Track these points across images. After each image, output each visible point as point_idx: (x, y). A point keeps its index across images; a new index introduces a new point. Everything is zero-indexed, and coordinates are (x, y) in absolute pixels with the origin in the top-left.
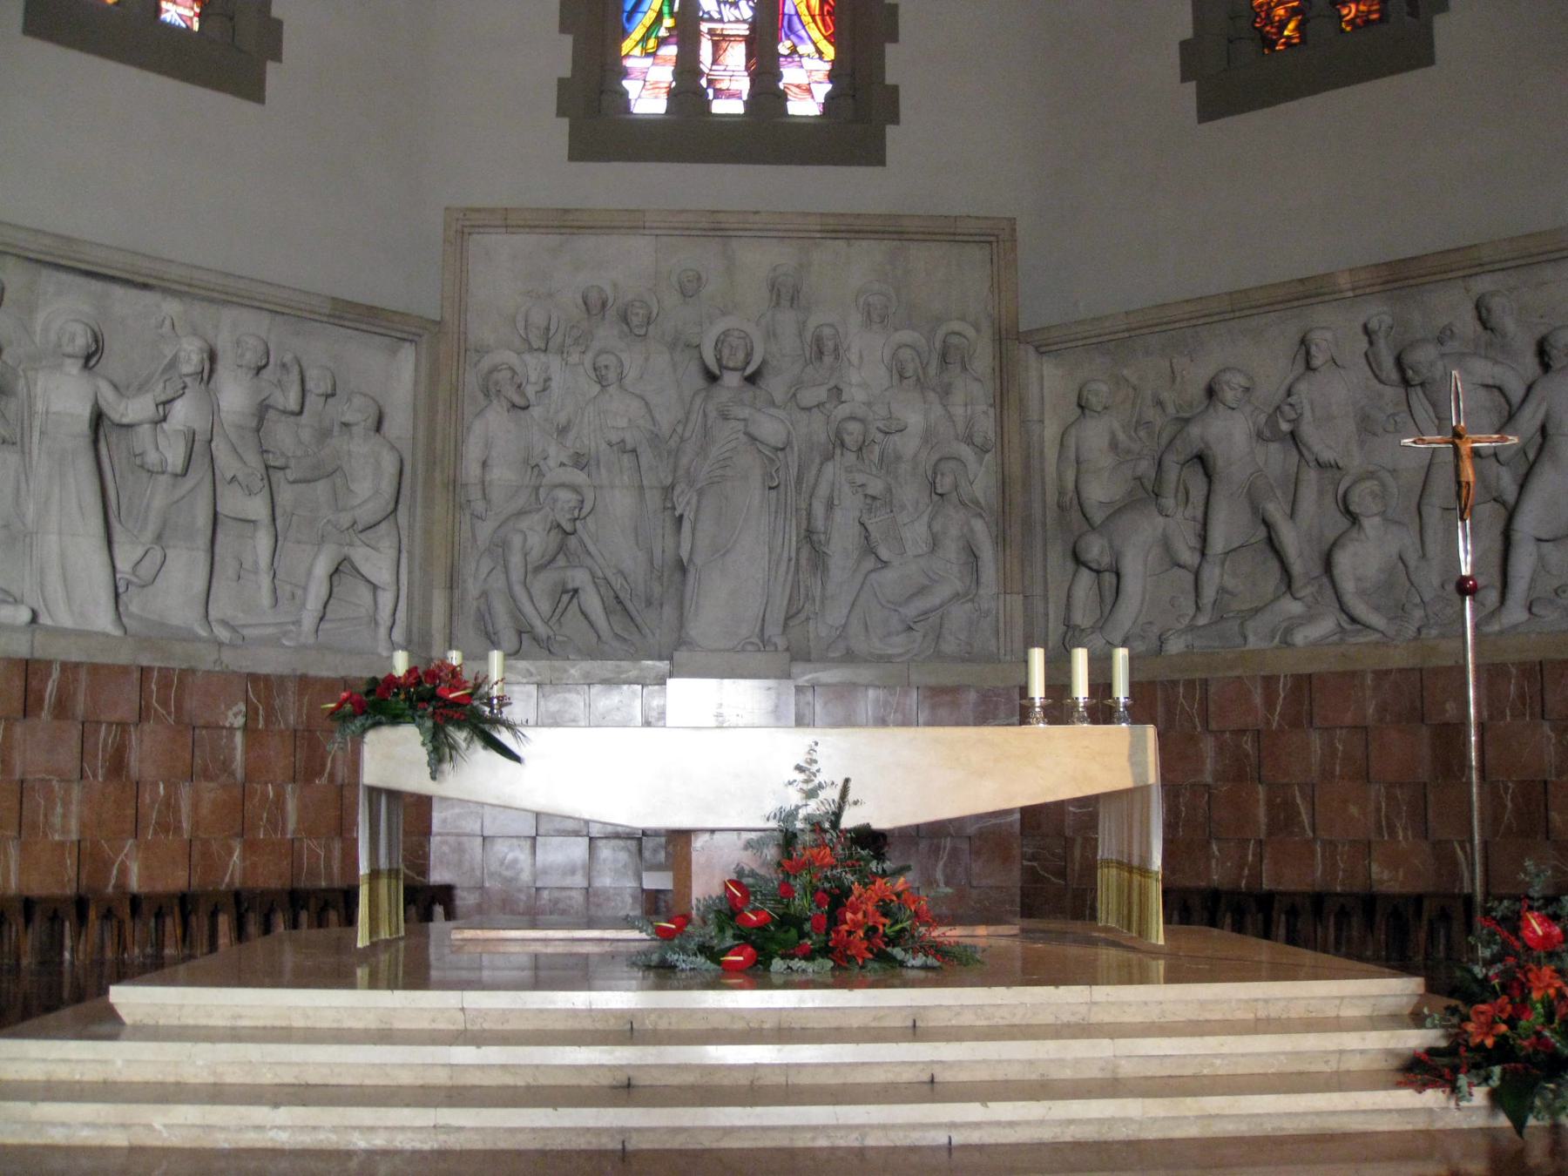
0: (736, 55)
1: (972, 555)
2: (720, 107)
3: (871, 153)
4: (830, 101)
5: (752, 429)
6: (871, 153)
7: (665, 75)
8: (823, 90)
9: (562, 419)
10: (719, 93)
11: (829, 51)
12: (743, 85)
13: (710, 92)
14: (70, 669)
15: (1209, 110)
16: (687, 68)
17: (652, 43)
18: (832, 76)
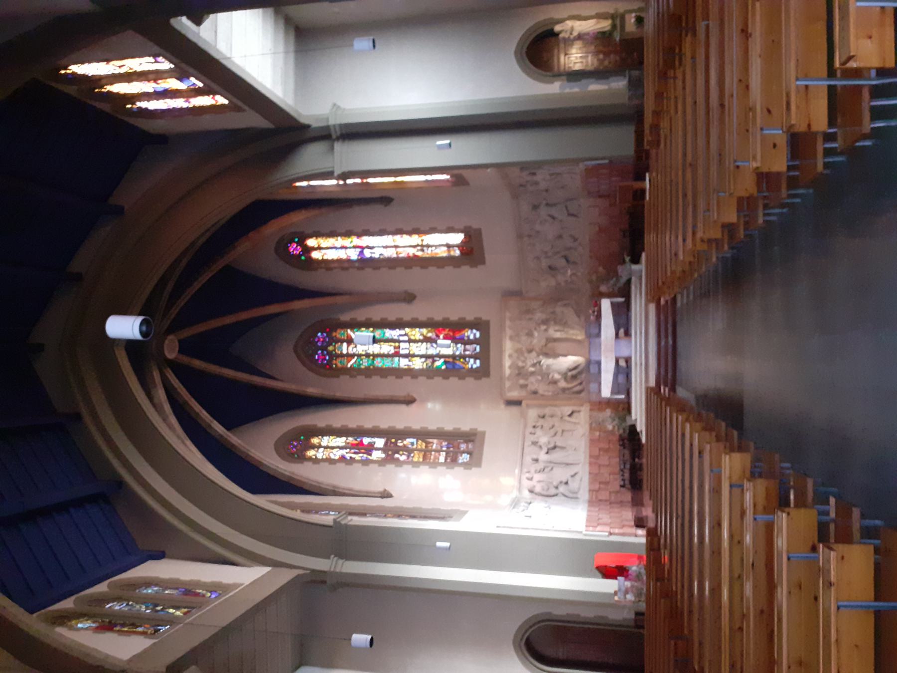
0: (468, 347)
1: (565, 305)
2: (478, 349)
3: (487, 323)
4: (477, 330)
5: (544, 344)
6: (487, 323)
7: (472, 361)
8: (474, 331)
9: (540, 378)
10: (475, 349)
11: (467, 329)
12: (475, 345)
13: (475, 352)
14: (591, 456)
15: (482, 261)
16: (470, 357)
17: (466, 363)
18: (472, 329)
